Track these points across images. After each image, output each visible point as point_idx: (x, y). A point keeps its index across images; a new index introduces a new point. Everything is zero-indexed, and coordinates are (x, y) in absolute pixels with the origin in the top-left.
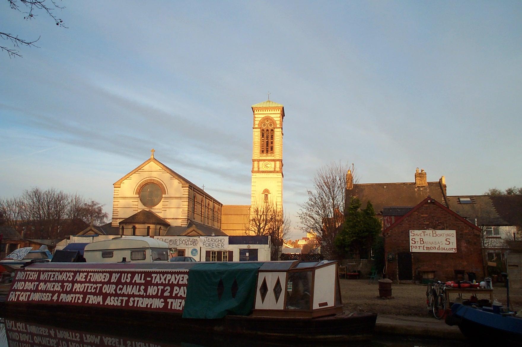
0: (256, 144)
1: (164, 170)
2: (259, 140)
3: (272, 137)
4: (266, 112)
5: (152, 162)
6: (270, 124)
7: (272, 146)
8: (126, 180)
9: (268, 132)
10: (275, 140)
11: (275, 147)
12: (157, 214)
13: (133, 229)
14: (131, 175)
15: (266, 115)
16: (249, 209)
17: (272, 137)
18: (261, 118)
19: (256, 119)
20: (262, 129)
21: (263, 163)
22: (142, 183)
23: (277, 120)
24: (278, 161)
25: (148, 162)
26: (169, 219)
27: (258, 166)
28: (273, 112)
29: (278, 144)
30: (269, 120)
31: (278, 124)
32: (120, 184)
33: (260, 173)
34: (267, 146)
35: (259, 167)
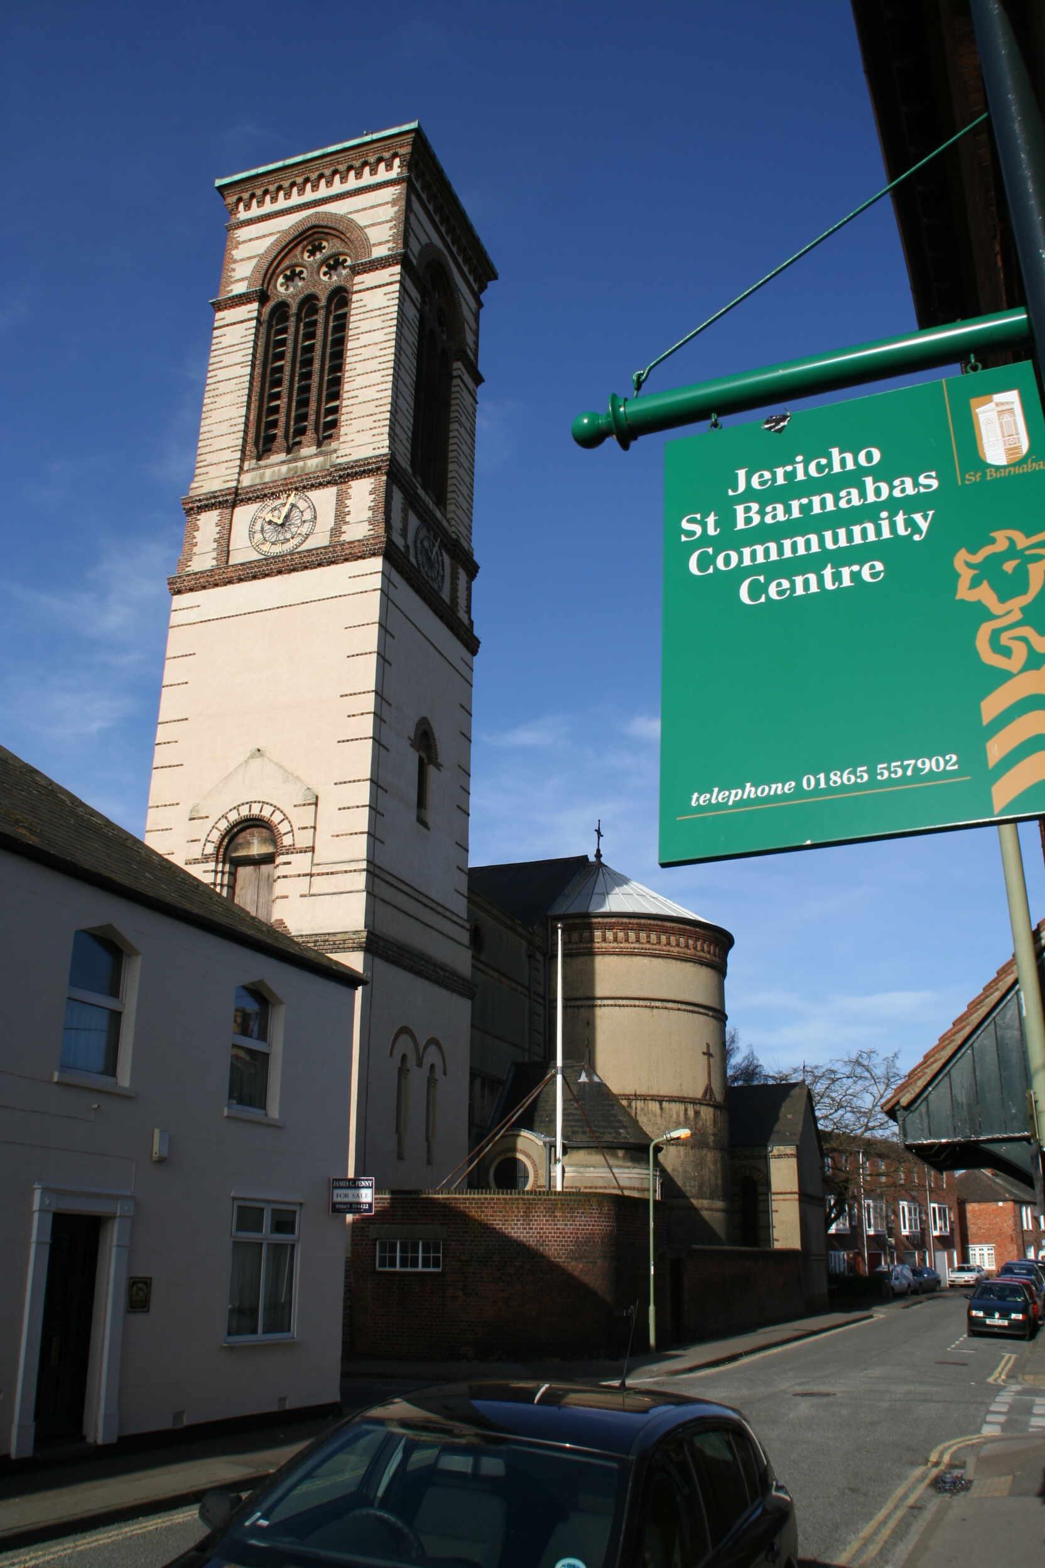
4: (309, 195)
23: (369, 226)
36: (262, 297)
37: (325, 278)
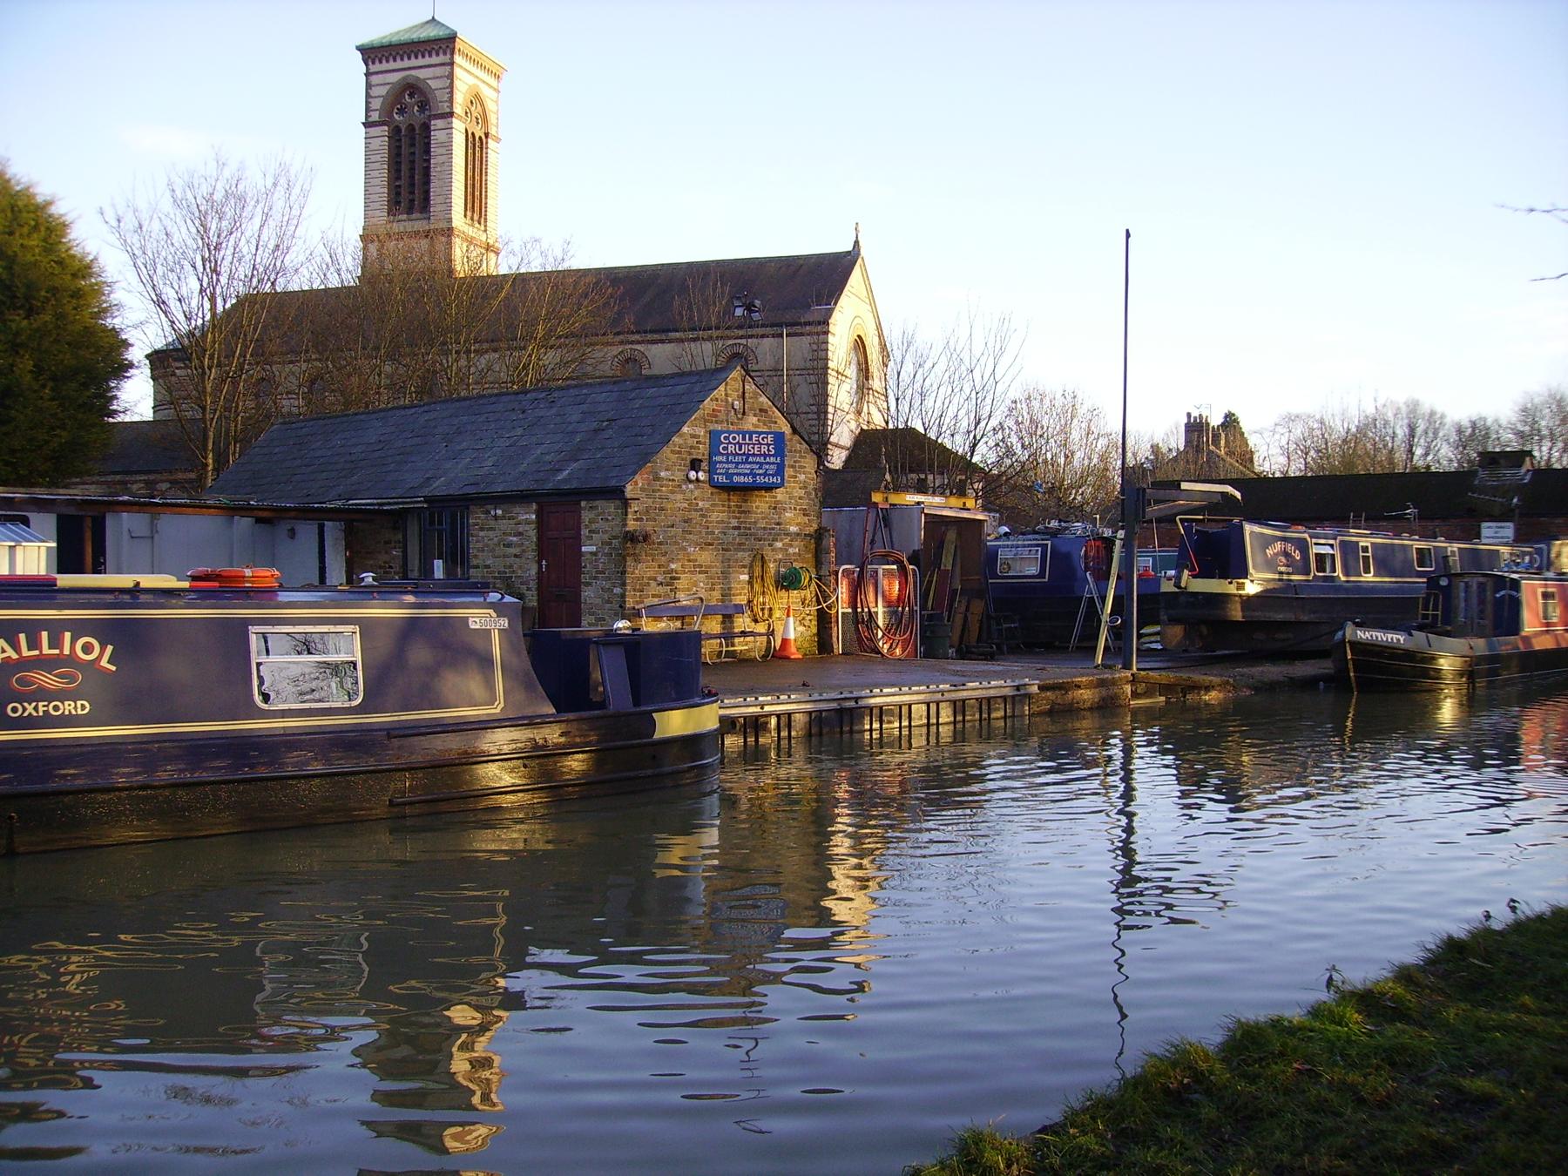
28: (427, 61)
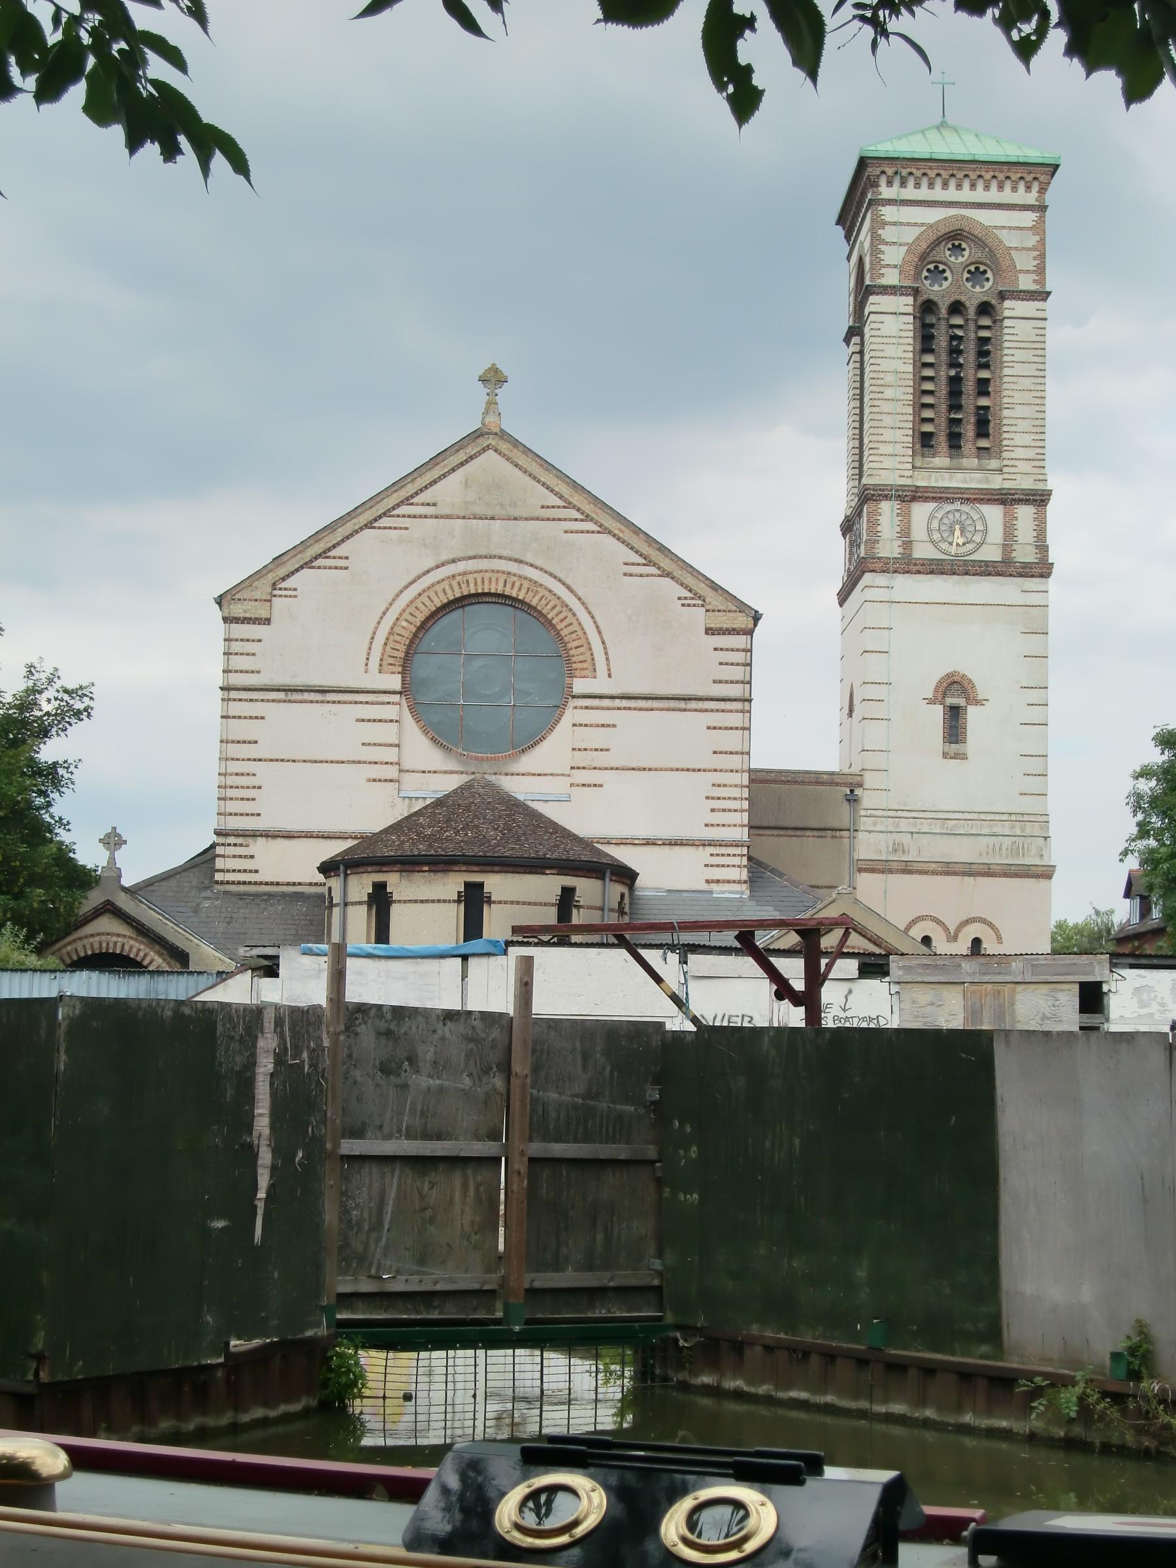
0: (889, 393)
1: (579, 516)
2: (910, 368)
3: (983, 354)
4: (952, 194)
5: (491, 451)
6: (972, 268)
7: (987, 408)
8: (305, 571)
9: (957, 320)
10: (1006, 371)
11: (1006, 413)
12: (530, 803)
13: (462, 906)
14: (343, 541)
15: (952, 212)
16: (852, 799)
17: (985, 353)
18: (917, 231)
19: (887, 234)
20: (921, 299)
21: (936, 510)
22: (424, 598)
24: (1027, 502)
25: (462, 456)
26: (622, 842)
27: (905, 533)
28: (993, 196)
29: (1027, 397)
30: (964, 245)
31: (1028, 272)
32: (270, 601)
33: (919, 572)
34: (955, 406)
35: (908, 535)
36: (916, 292)
37: (969, 285)
